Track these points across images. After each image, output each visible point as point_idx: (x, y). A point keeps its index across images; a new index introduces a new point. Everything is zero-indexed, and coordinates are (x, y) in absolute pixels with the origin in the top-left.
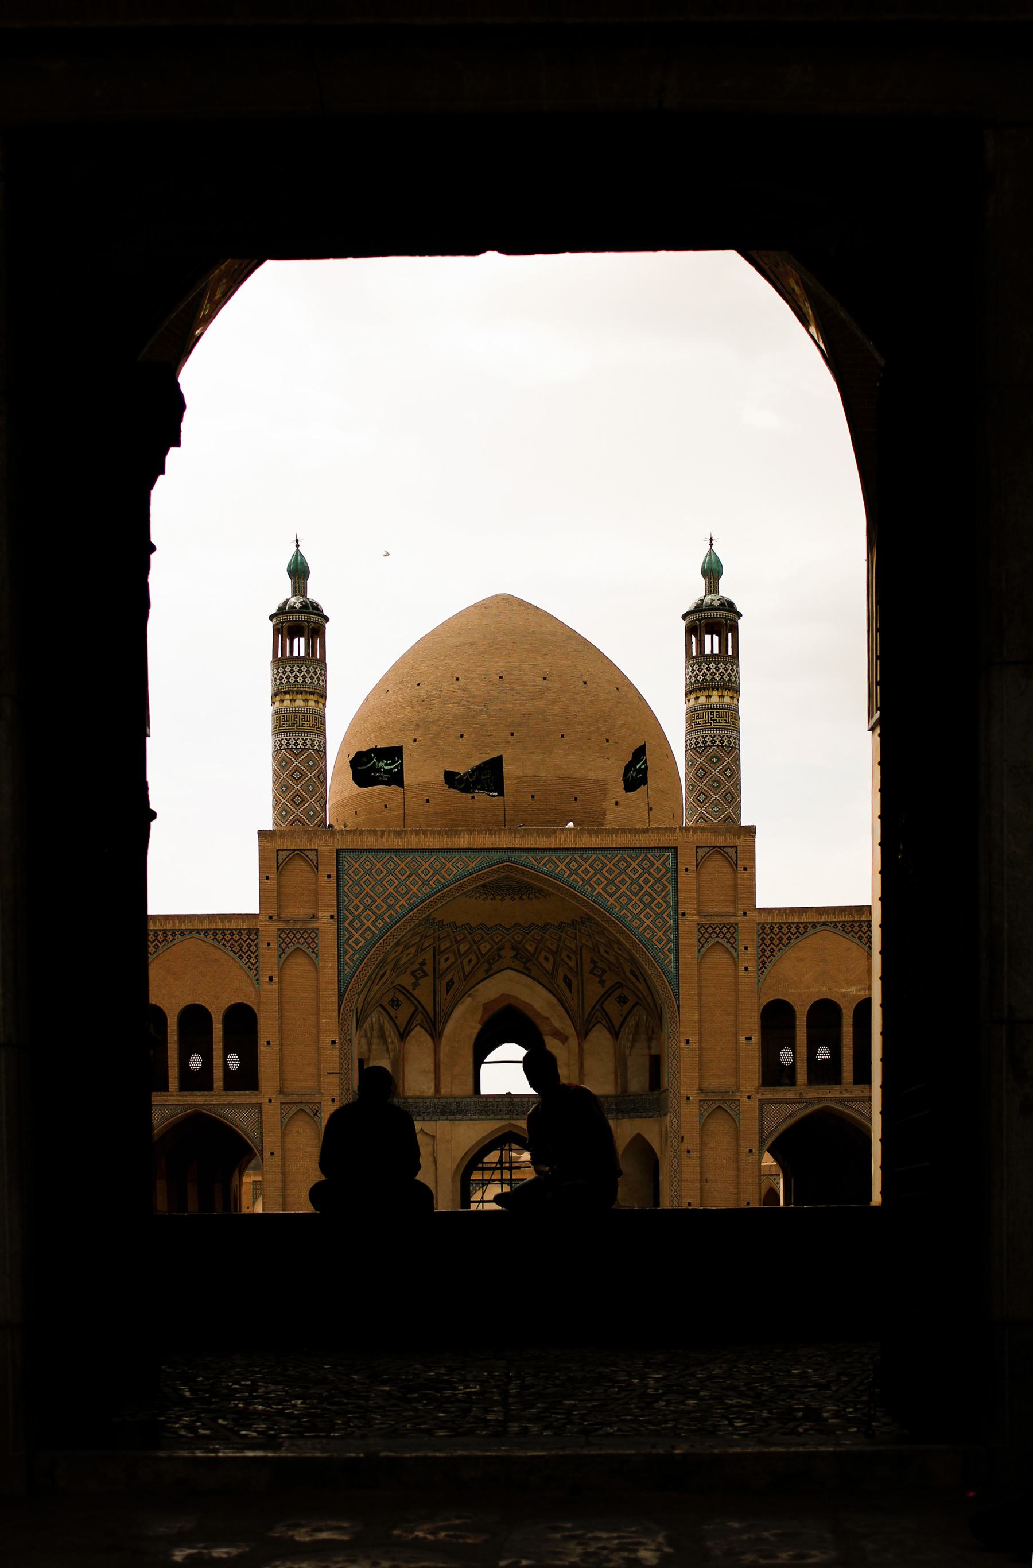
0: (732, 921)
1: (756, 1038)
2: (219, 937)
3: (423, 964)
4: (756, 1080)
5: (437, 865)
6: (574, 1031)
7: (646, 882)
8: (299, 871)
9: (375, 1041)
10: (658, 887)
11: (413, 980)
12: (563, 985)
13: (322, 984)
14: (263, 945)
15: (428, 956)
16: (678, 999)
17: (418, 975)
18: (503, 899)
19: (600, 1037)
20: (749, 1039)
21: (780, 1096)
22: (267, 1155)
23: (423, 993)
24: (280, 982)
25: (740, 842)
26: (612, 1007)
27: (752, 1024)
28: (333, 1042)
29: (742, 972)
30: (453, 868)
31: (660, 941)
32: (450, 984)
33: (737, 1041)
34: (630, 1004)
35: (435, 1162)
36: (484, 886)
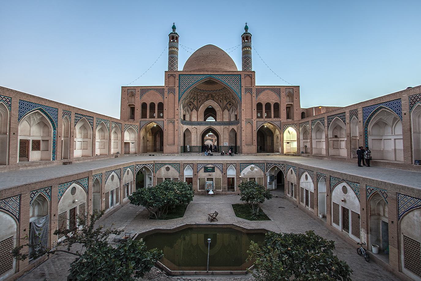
0: (251, 88)
1: (256, 109)
2: (157, 90)
3: (195, 97)
4: (256, 117)
5: (197, 77)
6: (221, 110)
7: (235, 81)
8: (172, 79)
9: (187, 112)
10: (237, 82)
11: (193, 100)
12: (220, 102)
13: (175, 98)
14: (165, 92)
15: (196, 96)
16: (241, 102)
17: (194, 99)
18: (209, 85)
19: (226, 111)
20: (254, 109)
21: (260, 120)
22: (164, 130)
23: (195, 103)
24: (168, 98)
25: (252, 74)
26: (228, 106)
27: (255, 107)
28: (177, 109)
29: (253, 97)
30: (200, 78)
31: (238, 91)
32: (200, 101)
33: (252, 110)
34: (231, 105)
35: (197, 133)
36: (206, 81)
